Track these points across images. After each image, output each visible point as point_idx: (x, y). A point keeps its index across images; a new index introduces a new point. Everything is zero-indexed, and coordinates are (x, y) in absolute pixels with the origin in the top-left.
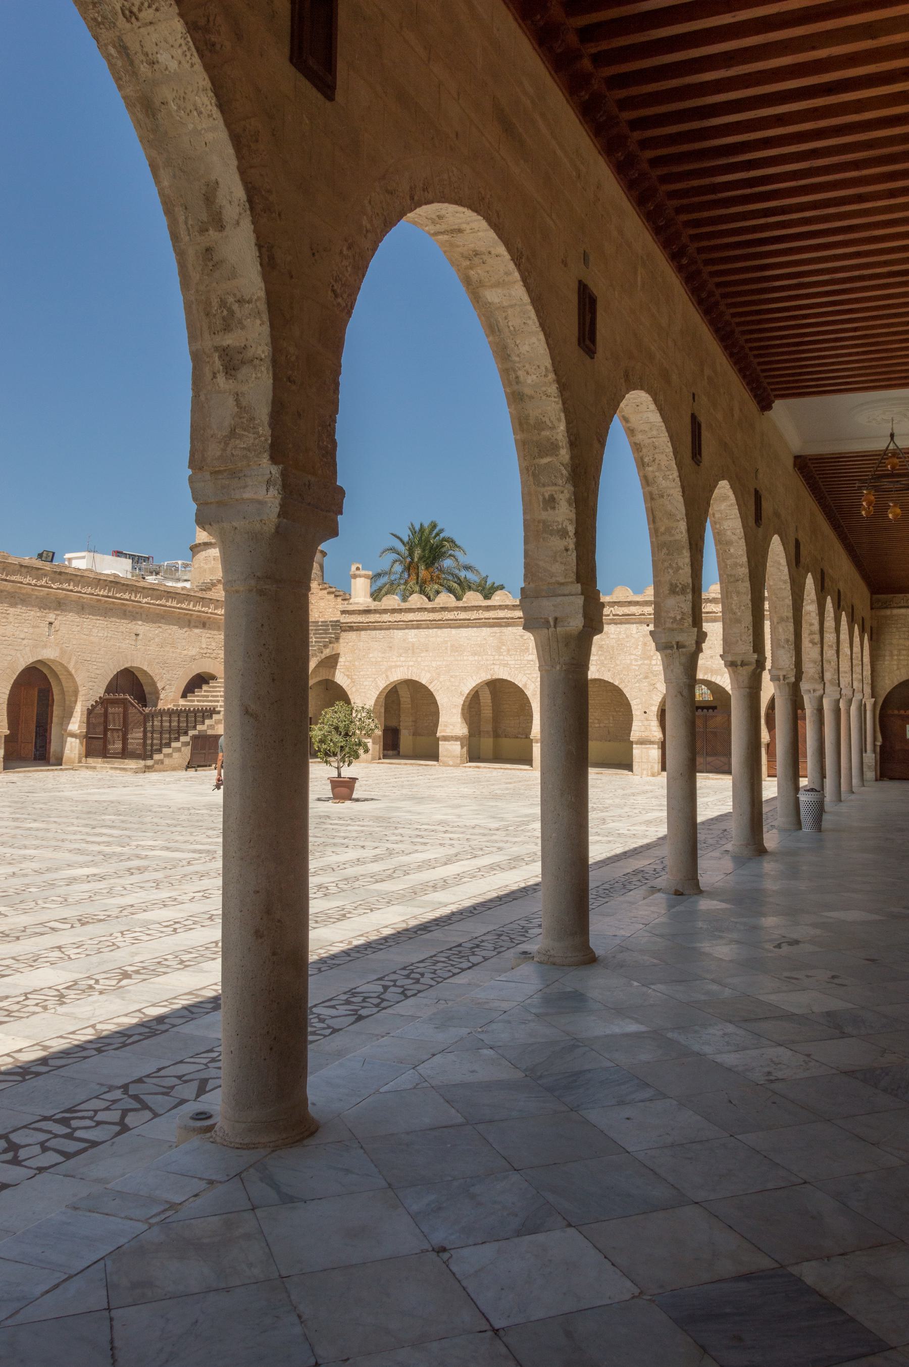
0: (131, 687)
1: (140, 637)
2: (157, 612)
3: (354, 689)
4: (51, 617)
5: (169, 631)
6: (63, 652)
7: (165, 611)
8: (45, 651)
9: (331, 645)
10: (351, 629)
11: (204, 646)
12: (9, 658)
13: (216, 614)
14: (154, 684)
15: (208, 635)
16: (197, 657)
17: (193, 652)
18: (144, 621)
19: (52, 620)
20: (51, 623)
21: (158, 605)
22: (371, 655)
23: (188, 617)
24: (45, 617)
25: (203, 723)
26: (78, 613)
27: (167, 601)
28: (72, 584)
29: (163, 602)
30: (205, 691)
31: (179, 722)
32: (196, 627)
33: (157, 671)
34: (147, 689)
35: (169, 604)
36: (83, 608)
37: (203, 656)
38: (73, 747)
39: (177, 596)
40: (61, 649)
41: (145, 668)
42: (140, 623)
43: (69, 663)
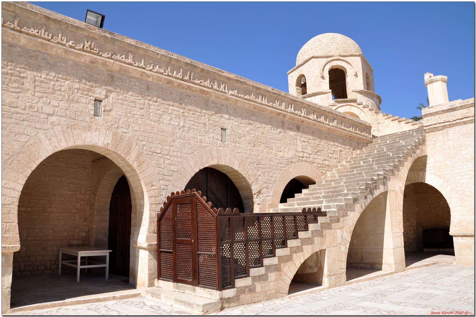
0: (219, 187)
1: (228, 132)
2: (246, 106)
3: (449, 189)
4: (100, 92)
5: (262, 130)
6: (118, 139)
7: (255, 108)
8: (89, 134)
9: (420, 147)
10: (436, 129)
11: (300, 149)
12: (24, 139)
13: (308, 118)
14: (248, 188)
15: (302, 139)
16: (294, 160)
17: (290, 154)
18: (230, 115)
19: (101, 97)
20: (98, 101)
21: (246, 99)
22: (464, 152)
23: (281, 117)
24: (89, 90)
25: (306, 229)
26: (141, 93)
27: (257, 97)
28: (131, 57)
29: (252, 97)
30: (305, 194)
31: (273, 228)
32: (291, 129)
33: (251, 172)
34: (243, 194)
35: (259, 100)
36: (148, 89)
37: (301, 159)
38: (144, 263)
39: (267, 94)
40: (115, 134)
41: (236, 168)
42: (226, 116)
43: (128, 153)
